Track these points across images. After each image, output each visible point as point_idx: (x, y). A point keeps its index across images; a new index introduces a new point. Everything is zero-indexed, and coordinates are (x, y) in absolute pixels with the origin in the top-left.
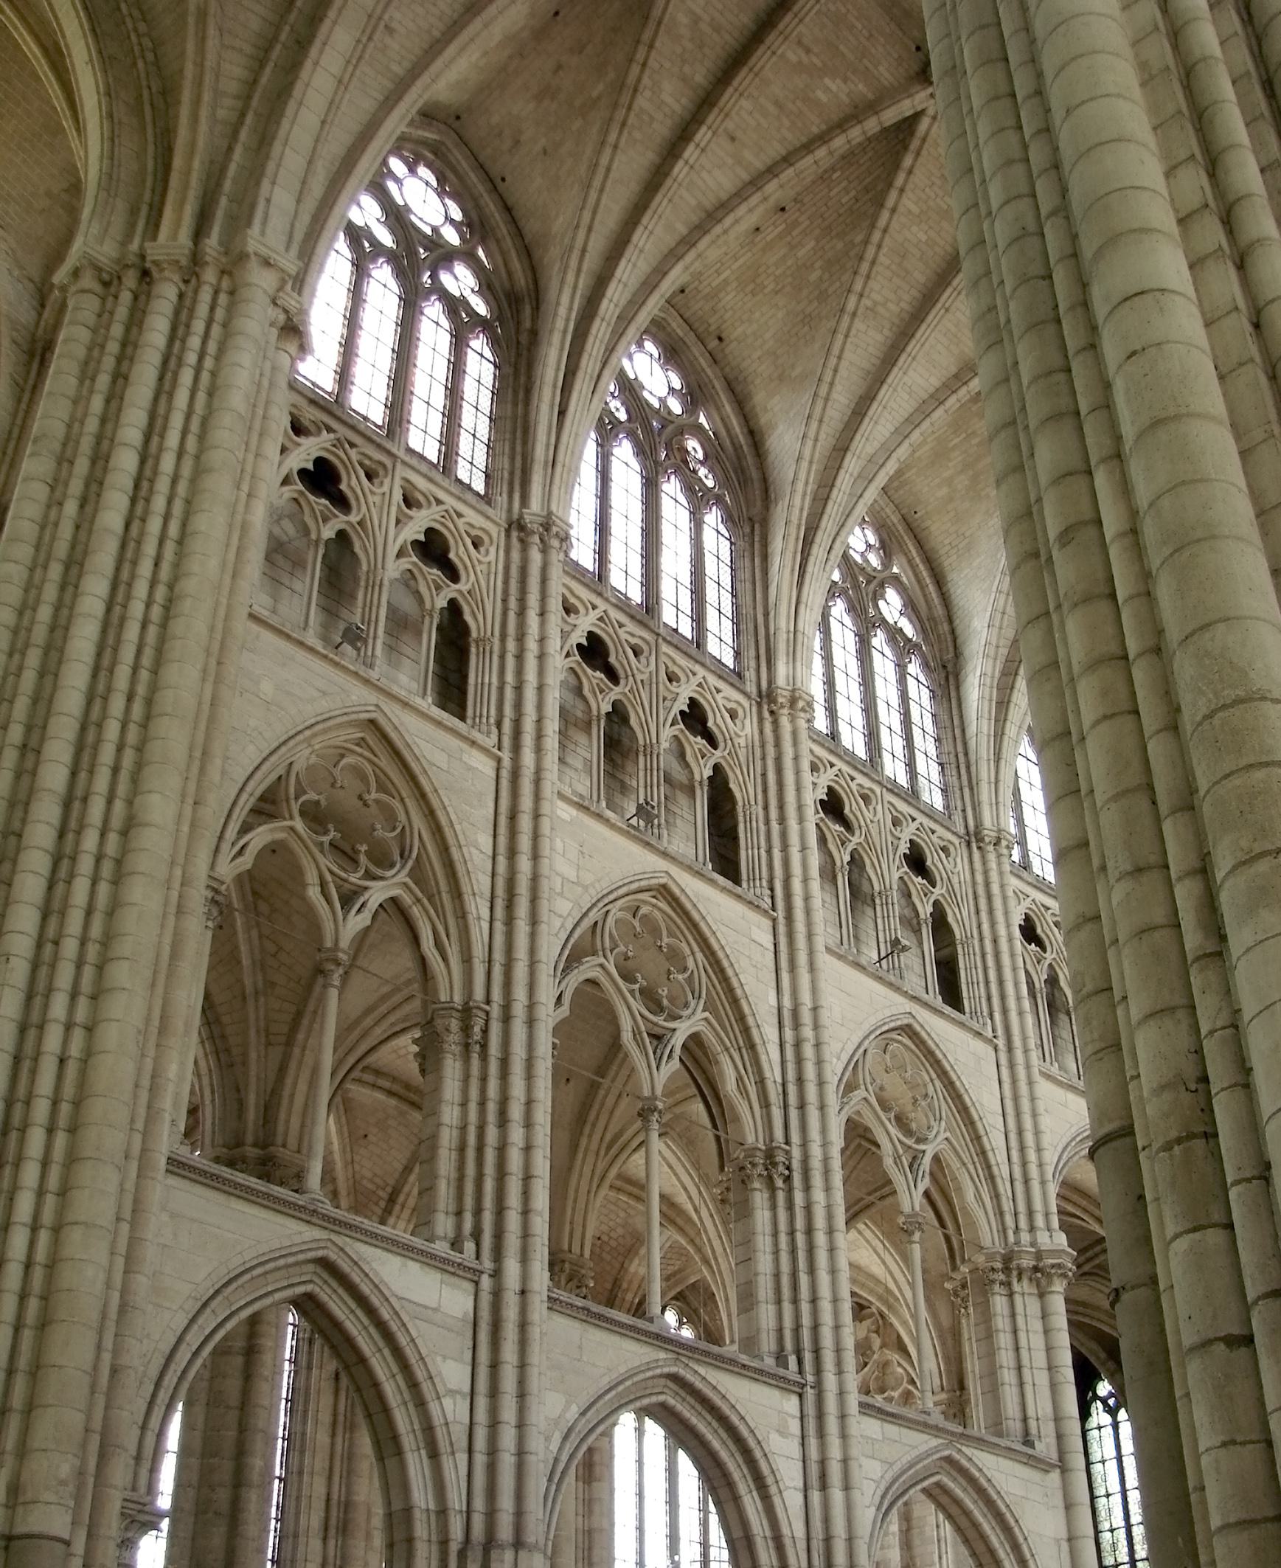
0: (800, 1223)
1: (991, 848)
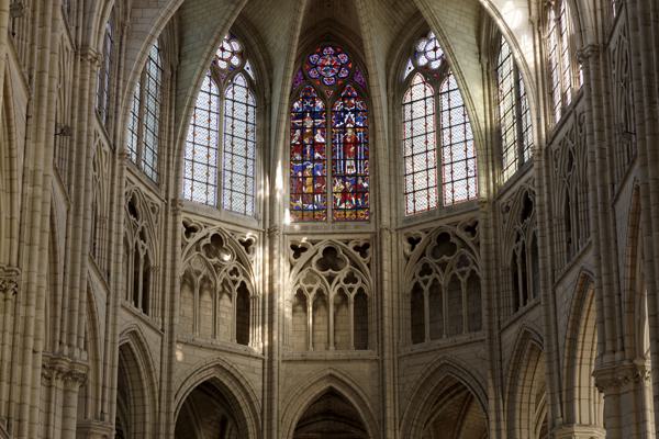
0: (20, 329)
1: (89, 63)
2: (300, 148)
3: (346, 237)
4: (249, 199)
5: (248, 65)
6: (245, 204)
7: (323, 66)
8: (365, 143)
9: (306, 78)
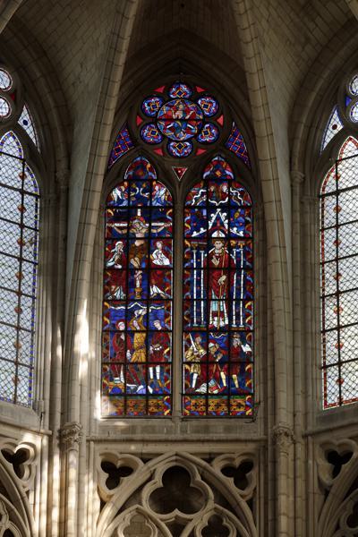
2: (121, 276)
3: (207, 448)
4: (24, 371)
5: (25, 116)
6: (16, 381)
7: (169, 119)
8: (246, 268)
9: (136, 142)
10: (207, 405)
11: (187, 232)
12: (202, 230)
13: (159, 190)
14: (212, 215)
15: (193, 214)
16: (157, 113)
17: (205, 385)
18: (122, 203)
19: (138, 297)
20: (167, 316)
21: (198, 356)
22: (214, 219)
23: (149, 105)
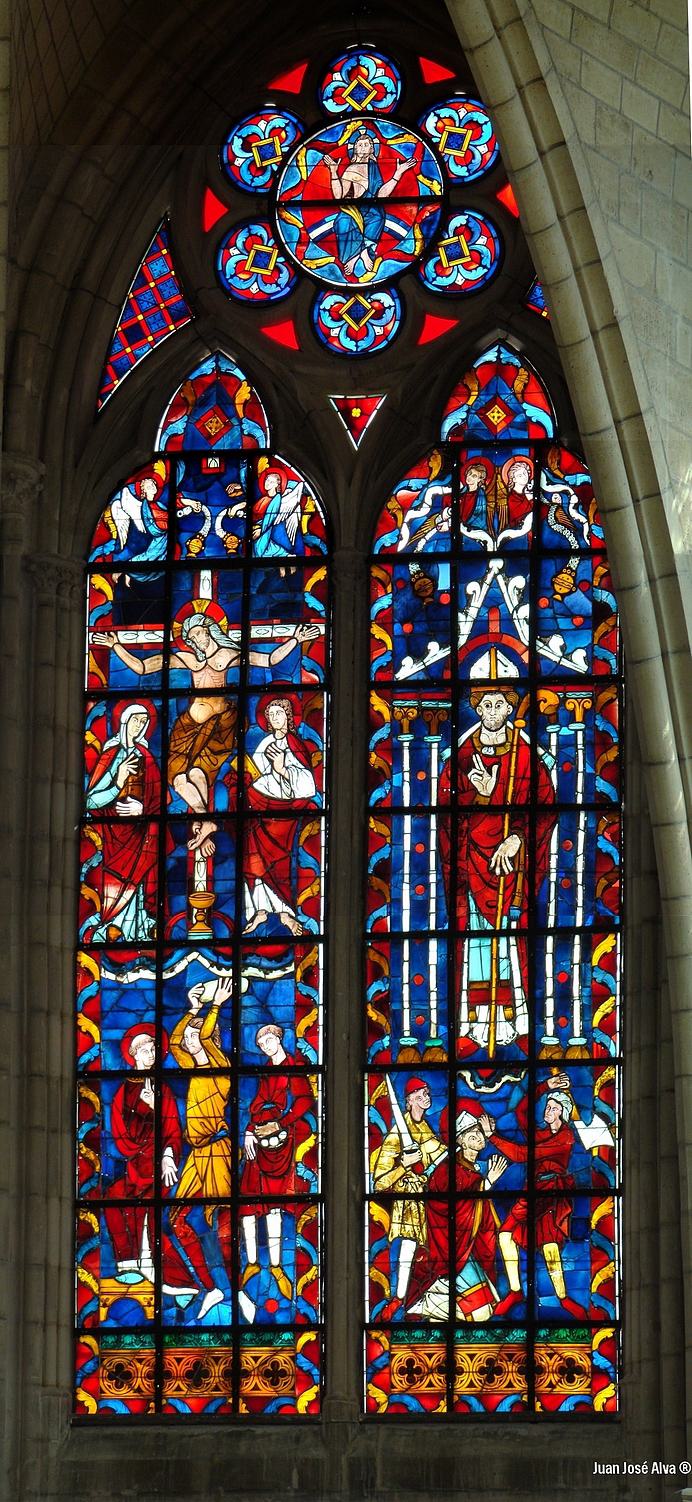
7: (318, 203)
8: (597, 805)
10: (450, 1369)
11: (380, 661)
12: (436, 652)
13: (280, 491)
14: (472, 587)
15: (402, 586)
16: (275, 176)
17: (441, 1285)
18: (143, 550)
19: (200, 932)
20: (304, 1006)
21: (418, 1168)
22: (477, 603)
23: (246, 147)
